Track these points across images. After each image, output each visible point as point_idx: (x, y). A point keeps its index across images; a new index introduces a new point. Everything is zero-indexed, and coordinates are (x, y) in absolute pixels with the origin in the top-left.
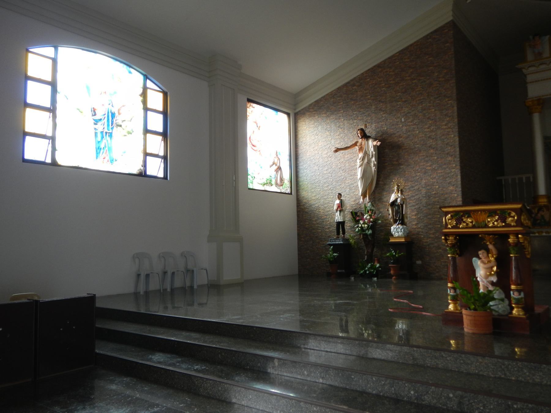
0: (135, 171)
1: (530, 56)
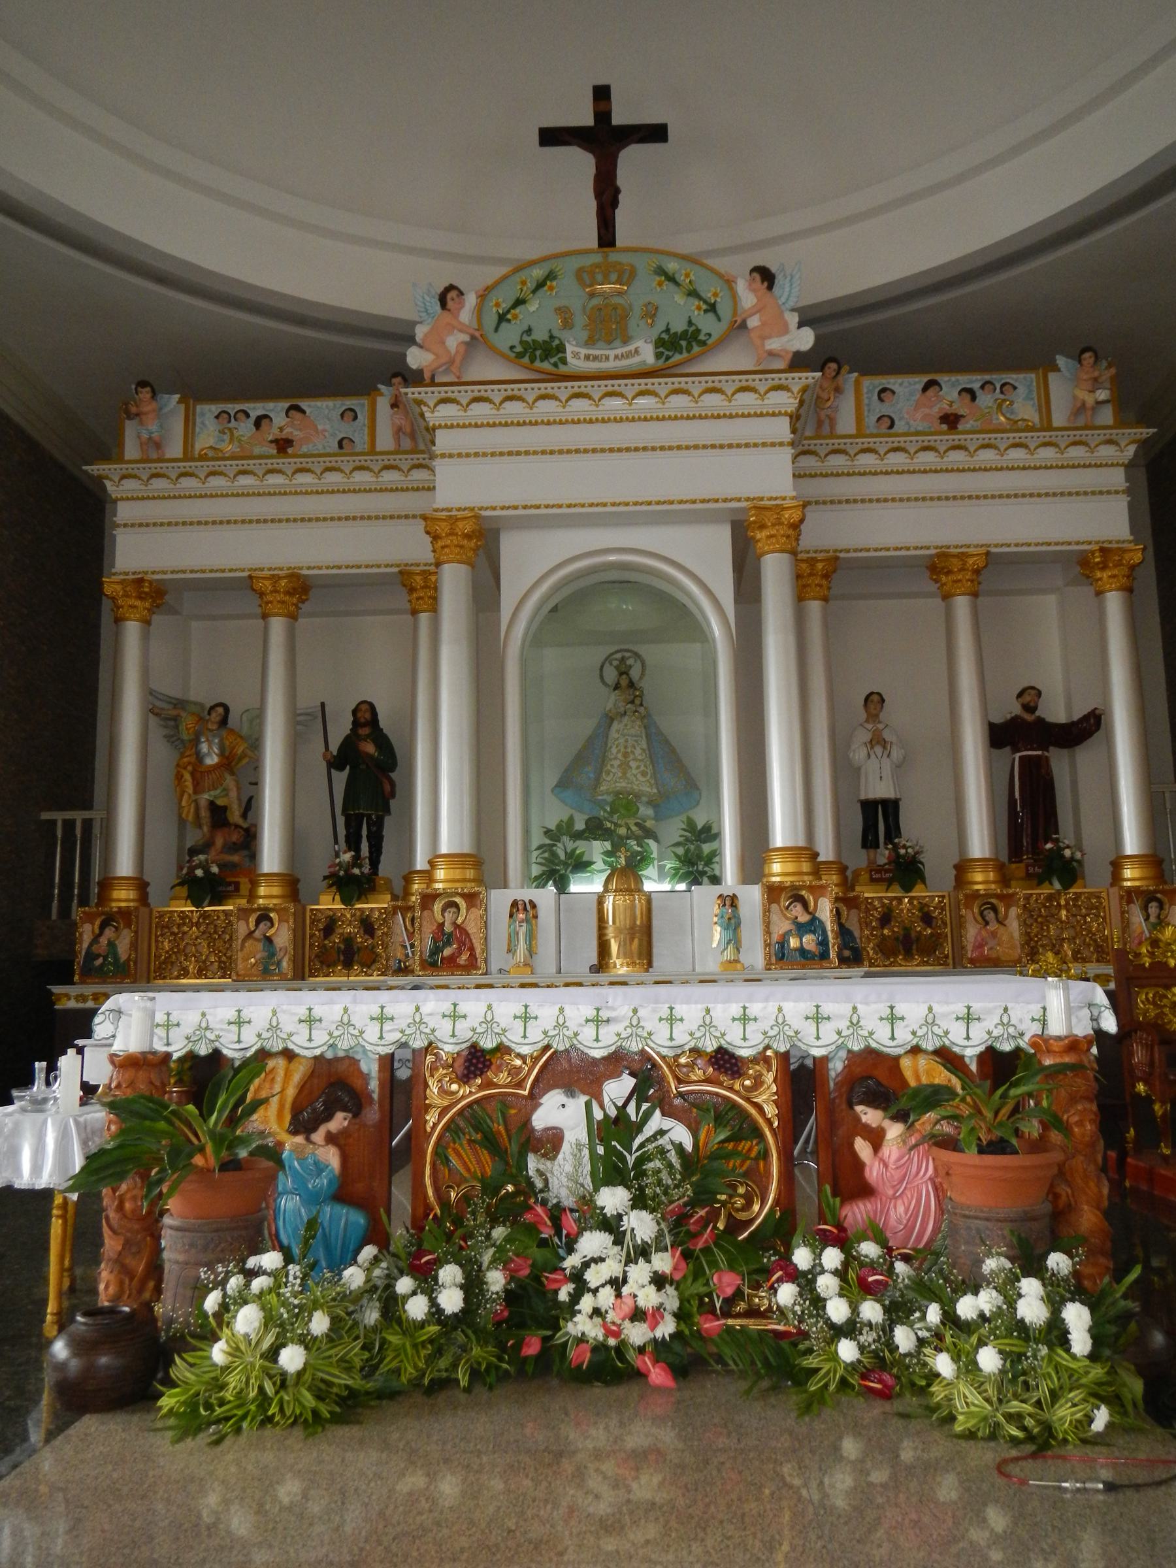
1: (131, 450)
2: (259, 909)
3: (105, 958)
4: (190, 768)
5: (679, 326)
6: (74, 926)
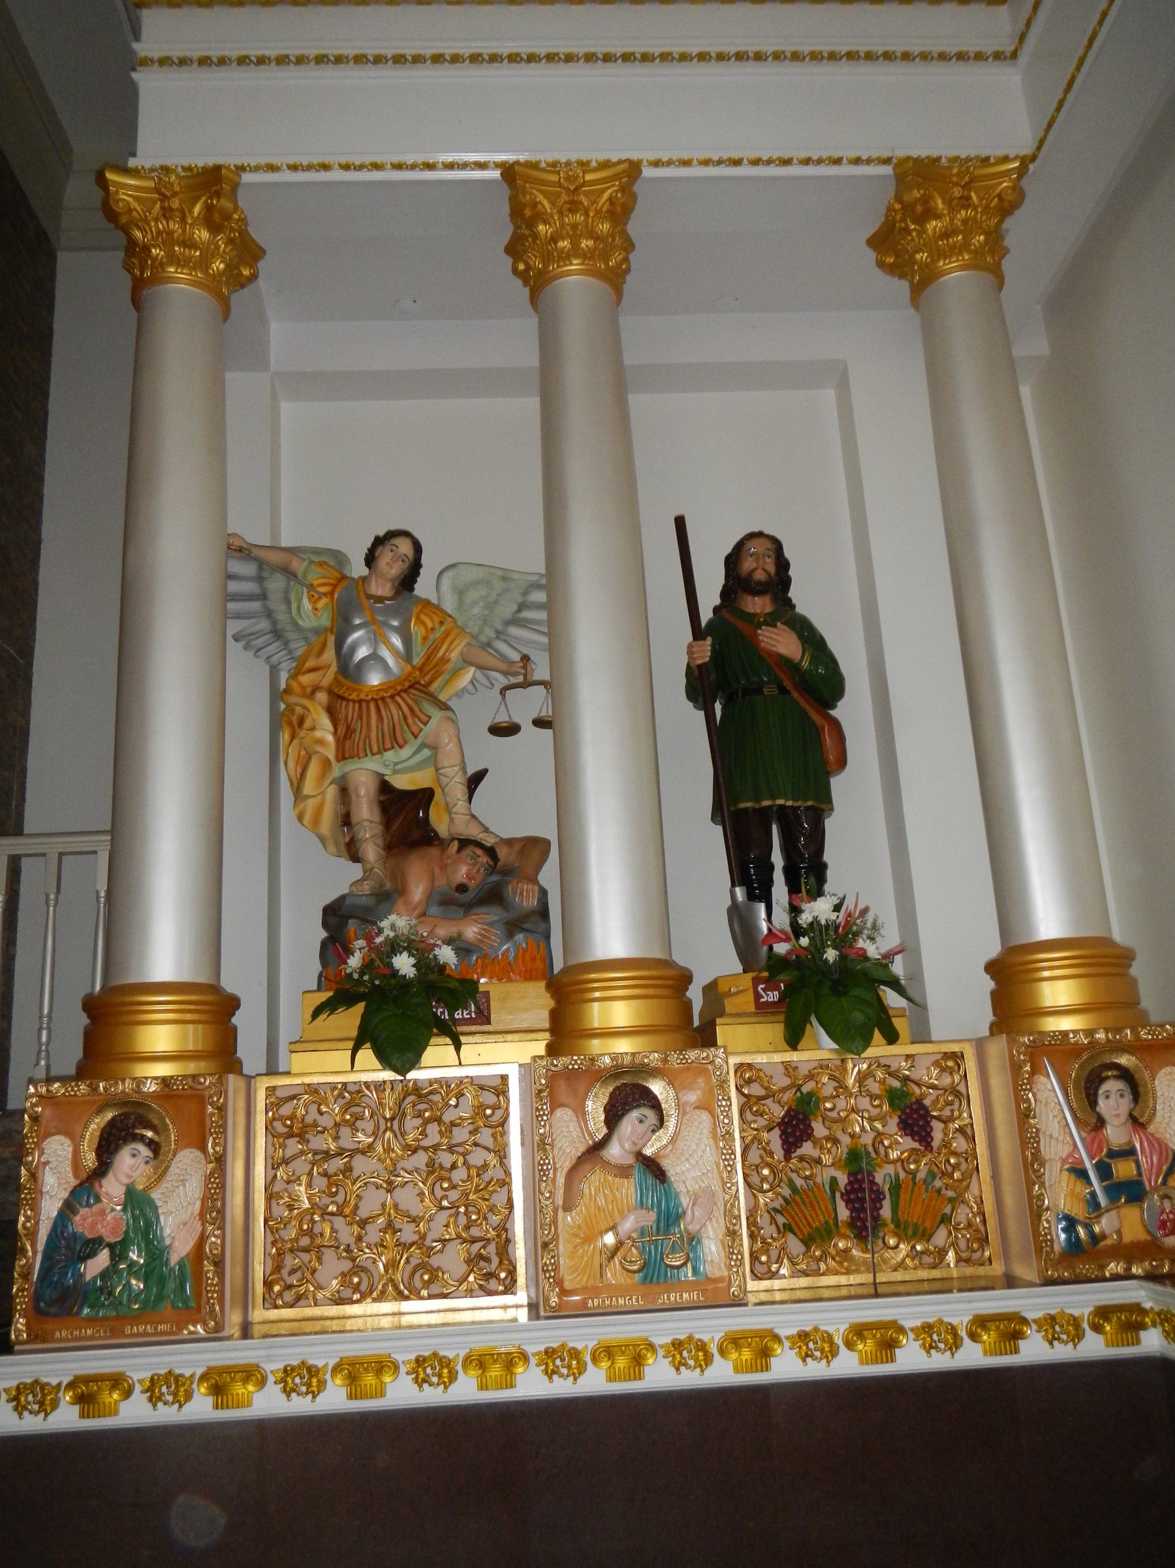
2: (617, 1071)
3: (118, 1252)
4: (322, 697)
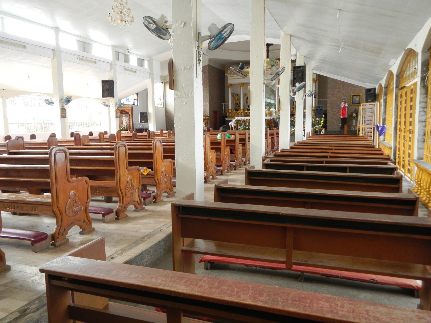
0: (132, 104)
1: (229, 72)
5: (273, 64)
6: (226, 113)
